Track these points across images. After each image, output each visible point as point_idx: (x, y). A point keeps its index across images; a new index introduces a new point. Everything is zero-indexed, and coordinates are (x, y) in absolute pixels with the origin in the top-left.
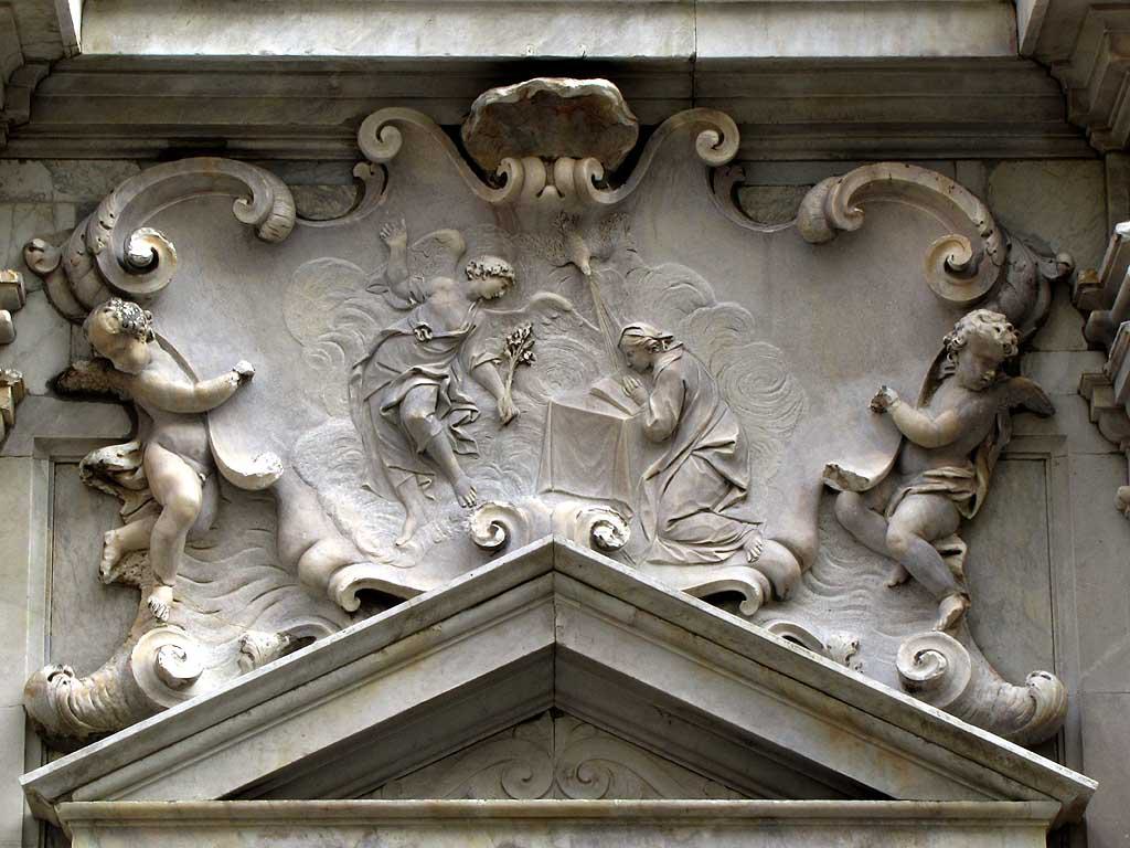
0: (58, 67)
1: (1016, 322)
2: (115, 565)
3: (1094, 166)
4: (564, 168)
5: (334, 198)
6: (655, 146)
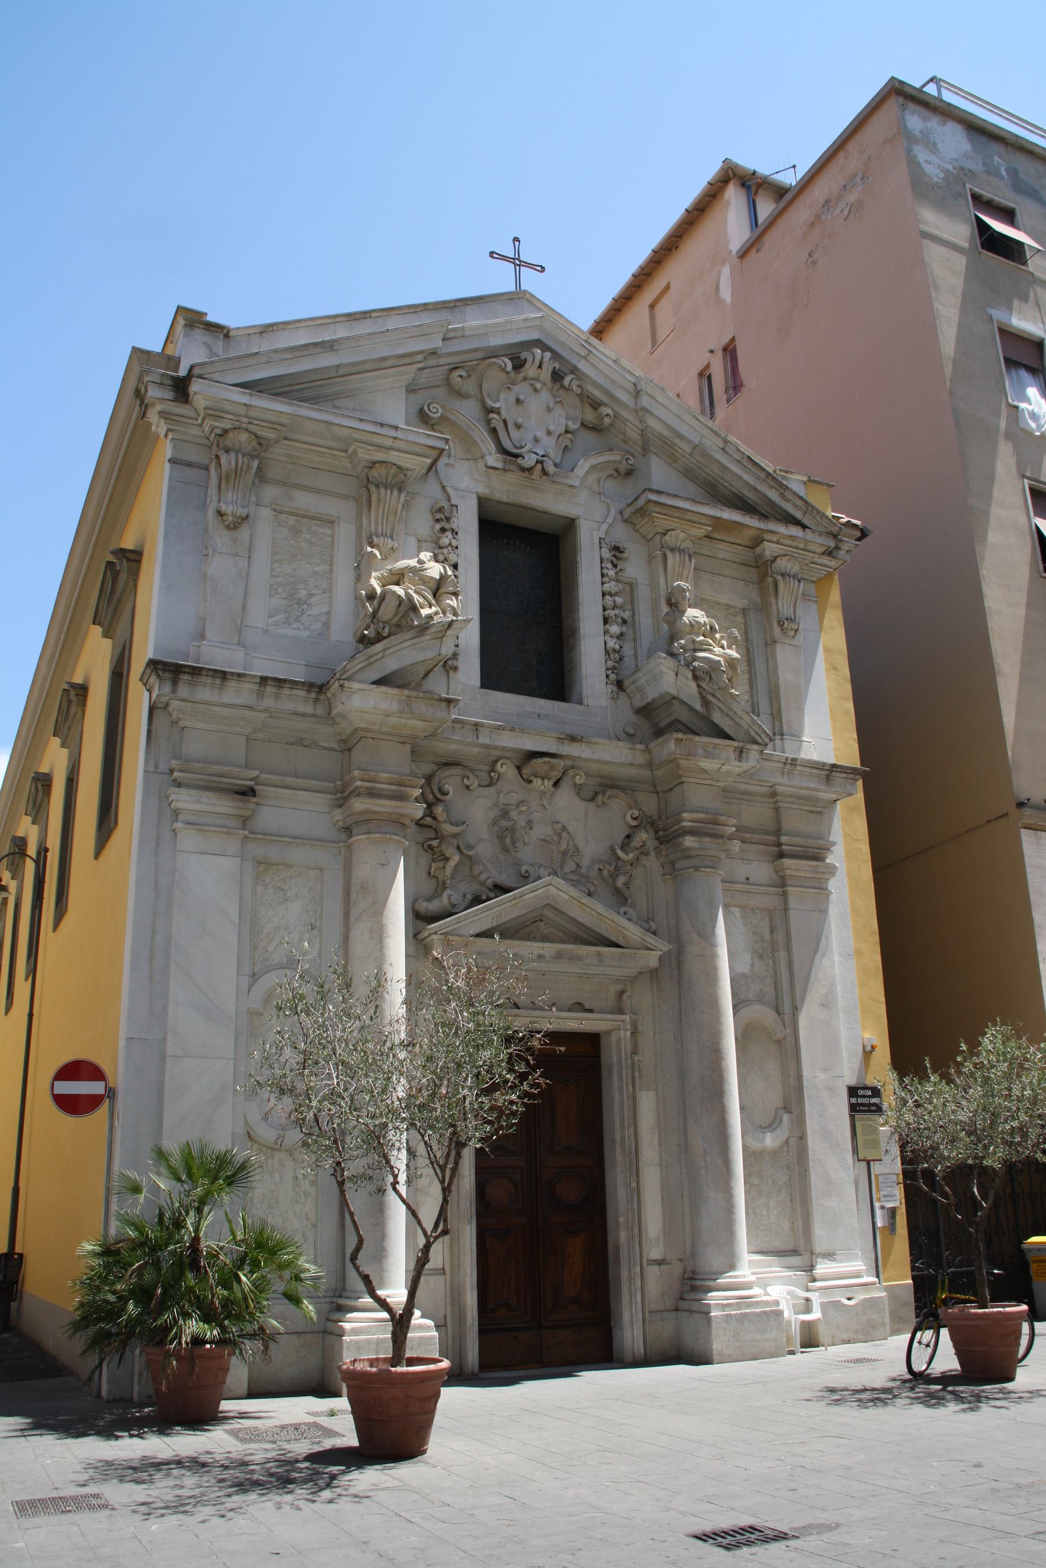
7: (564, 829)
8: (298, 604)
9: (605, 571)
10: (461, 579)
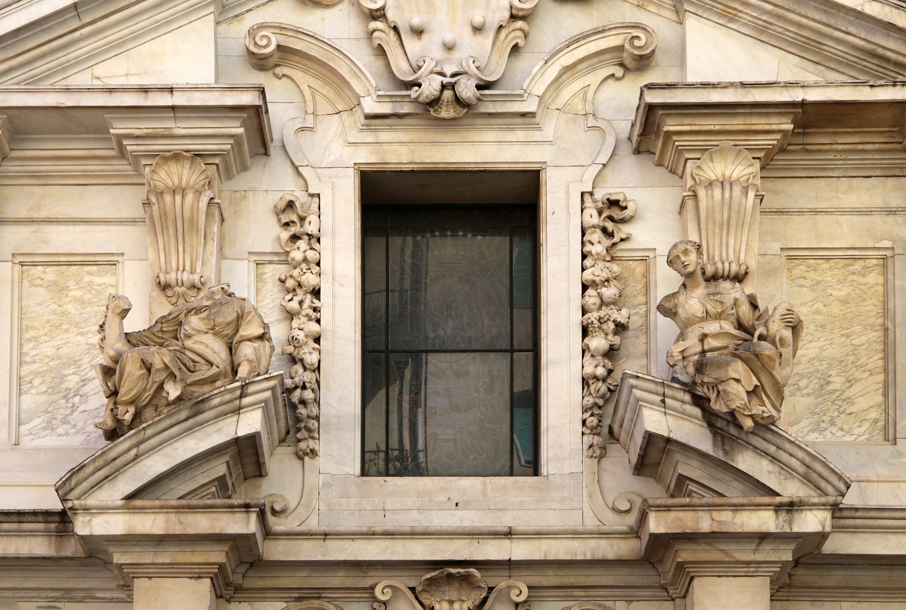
6: (493, 596)
8: (65, 397)
9: (588, 248)
10: (324, 316)
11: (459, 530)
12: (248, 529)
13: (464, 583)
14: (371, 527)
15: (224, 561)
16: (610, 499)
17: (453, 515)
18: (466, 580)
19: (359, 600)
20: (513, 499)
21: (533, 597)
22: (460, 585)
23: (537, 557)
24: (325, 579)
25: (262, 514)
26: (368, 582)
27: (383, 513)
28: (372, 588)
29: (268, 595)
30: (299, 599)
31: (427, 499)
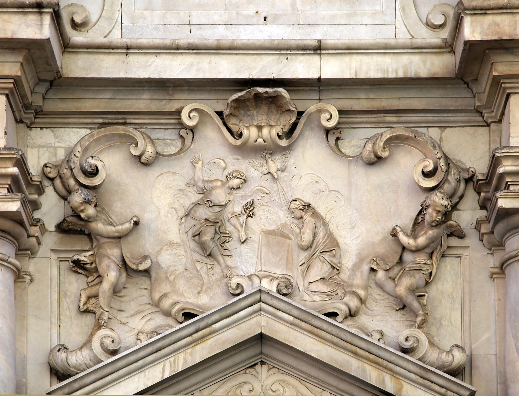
0: (54, 84)
1: (450, 197)
2: (85, 304)
3: (485, 130)
4: (265, 131)
5: (172, 145)
6: (302, 121)
7: (307, 207)
11: (267, 44)
12: (41, 33)
13: (273, 106)
14: (174, 40)
15: (19, 74)
16: (424, 11)
17: (261, 31)
18: (274, 101)
19: (165, 127)
20: (324, 13)
21: (344, 123)
22: (269, 108)
23: (347, 75)
24: (129, 102)
25: (56, 17)
26: (173, 106)
27: (188, 27)
28: (178, 113)
29: (70, 120)
30: (104, 125)
31: (234, 13)
